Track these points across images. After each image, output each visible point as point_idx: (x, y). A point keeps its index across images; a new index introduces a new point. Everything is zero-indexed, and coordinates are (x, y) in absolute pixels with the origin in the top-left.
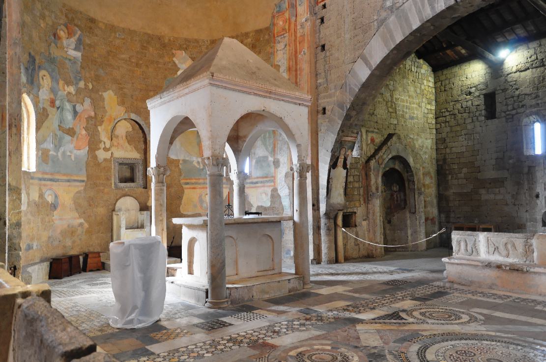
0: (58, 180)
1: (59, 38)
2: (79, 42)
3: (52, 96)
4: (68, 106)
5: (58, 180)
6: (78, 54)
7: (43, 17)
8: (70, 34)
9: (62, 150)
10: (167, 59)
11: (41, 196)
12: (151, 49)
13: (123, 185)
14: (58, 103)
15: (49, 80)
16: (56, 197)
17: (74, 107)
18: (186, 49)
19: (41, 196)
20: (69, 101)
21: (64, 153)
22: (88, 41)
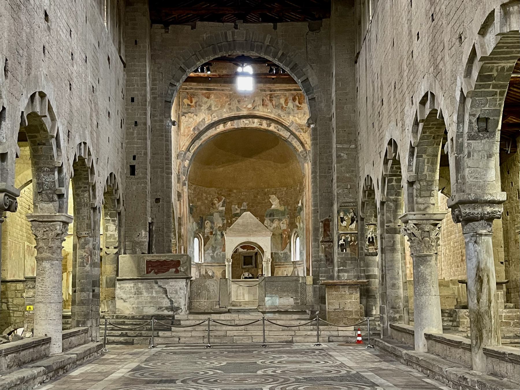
0: (214, 266)
1: (215, 204)
2: (224, 202)
3: (211, 230)
4: (219, 233)
5: (214, 266)
6: (224, 208)
7: (207, 199)
8: (219, 201)
9: (216, 252)
10: (266, 201)
11: (206, 273)
12: (259, 197)
13: (245, 267)
14: (214, 233)
15: (210, 224)
16: (213, 273)
17: (222, 232)
18: (275, 194)
19: (206, 273)
20: (219, 230)
21: (217, 254)
22: (228, 201)
